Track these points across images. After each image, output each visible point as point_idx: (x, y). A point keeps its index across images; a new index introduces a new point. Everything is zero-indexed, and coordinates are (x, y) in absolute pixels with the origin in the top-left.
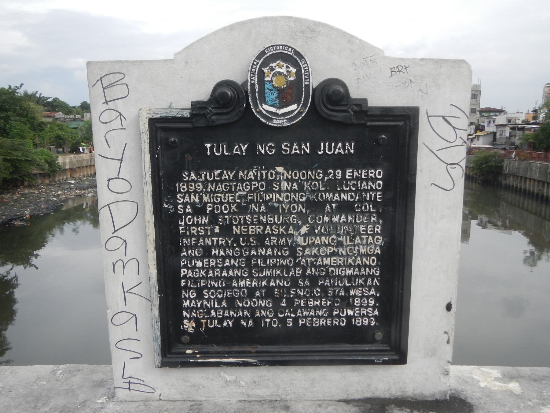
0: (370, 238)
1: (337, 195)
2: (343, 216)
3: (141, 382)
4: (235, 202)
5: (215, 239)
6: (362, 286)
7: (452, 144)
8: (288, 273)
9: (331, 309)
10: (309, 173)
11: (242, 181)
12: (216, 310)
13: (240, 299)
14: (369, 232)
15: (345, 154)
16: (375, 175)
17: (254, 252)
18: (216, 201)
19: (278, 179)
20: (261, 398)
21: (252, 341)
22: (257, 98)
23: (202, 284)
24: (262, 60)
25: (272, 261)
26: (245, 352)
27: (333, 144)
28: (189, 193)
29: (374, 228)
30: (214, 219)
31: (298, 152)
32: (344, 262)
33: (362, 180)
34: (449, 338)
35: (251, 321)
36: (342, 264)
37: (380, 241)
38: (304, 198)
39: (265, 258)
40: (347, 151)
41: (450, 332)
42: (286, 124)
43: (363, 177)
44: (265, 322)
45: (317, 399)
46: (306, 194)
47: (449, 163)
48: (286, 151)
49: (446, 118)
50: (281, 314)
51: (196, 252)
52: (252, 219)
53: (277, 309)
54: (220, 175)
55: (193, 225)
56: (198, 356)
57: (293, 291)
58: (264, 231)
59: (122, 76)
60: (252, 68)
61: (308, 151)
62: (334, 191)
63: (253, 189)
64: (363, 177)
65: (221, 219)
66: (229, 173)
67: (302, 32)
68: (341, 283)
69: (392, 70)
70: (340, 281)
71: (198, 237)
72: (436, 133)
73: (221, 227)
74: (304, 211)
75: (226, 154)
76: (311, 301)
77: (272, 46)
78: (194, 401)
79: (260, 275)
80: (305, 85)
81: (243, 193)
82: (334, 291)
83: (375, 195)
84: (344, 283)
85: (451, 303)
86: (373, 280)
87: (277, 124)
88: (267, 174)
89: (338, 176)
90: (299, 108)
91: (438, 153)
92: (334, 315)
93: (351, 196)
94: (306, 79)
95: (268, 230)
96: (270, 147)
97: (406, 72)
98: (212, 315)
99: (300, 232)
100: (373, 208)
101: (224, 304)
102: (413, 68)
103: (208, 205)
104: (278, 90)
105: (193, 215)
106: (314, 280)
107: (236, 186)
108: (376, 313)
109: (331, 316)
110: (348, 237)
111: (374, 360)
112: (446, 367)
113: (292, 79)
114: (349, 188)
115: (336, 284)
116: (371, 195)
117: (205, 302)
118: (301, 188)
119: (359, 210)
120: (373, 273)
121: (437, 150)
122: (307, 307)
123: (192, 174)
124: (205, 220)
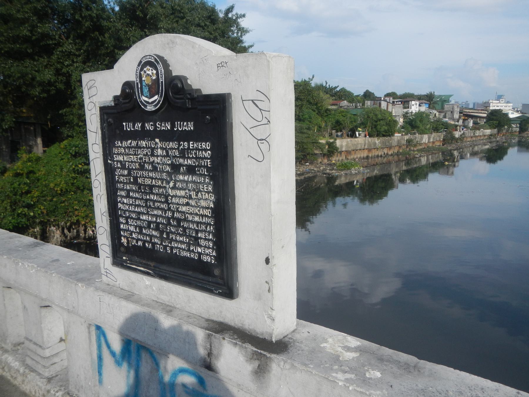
0: (207, 194)
1: (186, 160)
2: (190, 176)
3: (111, 273)
4: (138, 162)
5: (131, 186)
6: (205, 231)
7: (260, 123)
8: (165, 214)
9: (189, 244)
10: (171, 143)
11: (140, 148)
12: (135, 232)
13: (145, 228)
14: (205, 190)
15: (189, 130)
16: (206, 146)
17: (148, 197)
18: (130, 161)
19: (156, 147)
20: (164, 302)
21: (153, 259)
22: (140, 92)
23: (128, 215)
24: (140, 66)
25: (157, 204)
26: (148, 265)
27: (182, 123)
28: (118, 154)
29: (207, 186)
31: (164, 128)
32: (193, 211)
33: (199, 150)
34: (269, 288)
35: (150, 245)
36: (192, 212)
37: (213, 198)
38: (170, 162)
39: (154, 201)
40: (189, 128)
41: (270, 283)
42: (154, 109)
43: (199, 148)
44: (157, 247)
45: (192, 313)
46: (170, 159)
47: (259, 139)
48: (159, 128)
49: (254, 101)
50: (164, 243)
51: (124, 193)
52: (146, 174)
54: (131, 144)
55: (121, 175)
56: (128, 262)
57: (169, 227)
58: (152, 182)
59: (93, 82)
60: (136, 72)
61: (169, 128)
62: (183, 157)
63: (145, 153)
64: (199, 148)
65: (132, 172)
66: (134, 142)
67: (168, 44)
68: (193, 226)
69: (218, 65)
70: (192, 225)
71: (124, 183)
72: (249, 114)
73: (133, 177)
74: (170, 171)
75: (132, 129)
76: (178, 237)
77: (144, 57)
78: (133, 293)
79: (152, 213)
80: (161, 82)
81: (142, 156)
82: (190, 232)
83: (207, 162)
84: (194, 227)
85: (269, 258)
86: (210, 228)
87: (149, 109)
88: (151, 143)
89: (186, 147)
90: (159, 98)
91: (251, 130)
92: (191, 250)
93: (194, 161)
94: (161, 77)
95: (154, 183)
96: (151, 125)
97: (226, 66)
98: (133, 236)
99: (170, 186)
100: (207, 172)
101: (137, 230)
102: (230, 62)
103: (127, 163)
104: (148, 86)
105: (121, 169)
106: (179, 221)
107: (138, 151)
108: (214, 254)
109: (189, 250)
110: (194, 192)
111: (213, 290)
112: (270, 313)
113: (154, 78)
114: (192, 156)
115: (190, 227)
116: (204, 162)
117: (130, 227)
118: (167, 155)
119: (199, 173)
120: (210, 222)
121: (250, 128)
122: (176, 241)
123: (119, 143)
124: (126, 172)
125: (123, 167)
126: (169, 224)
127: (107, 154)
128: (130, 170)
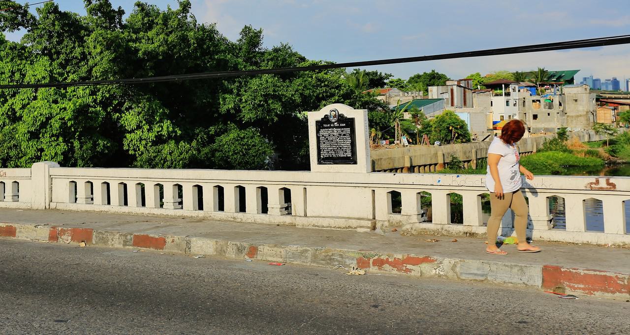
30: (325, 137)
53: (335, 153)
106: (341, 148)
125: (323, 136)
126: (338, 149)
127: (318, 131)
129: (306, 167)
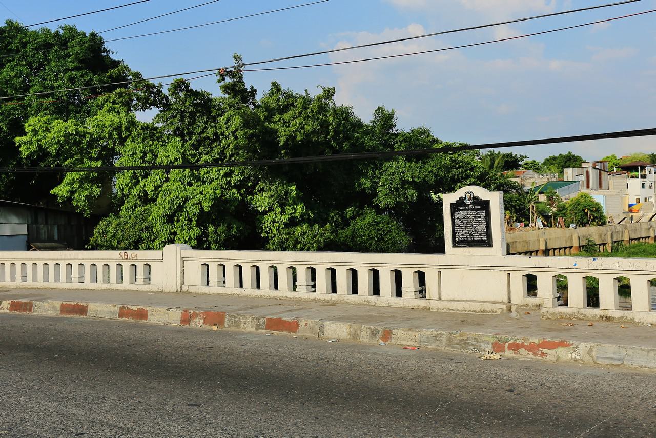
53: (470, 236)
106: (476, 230)
125: (458, 218)
126: (473, 232)
127: (453, 214)
128: (460, 219)
129: (441, 250)
